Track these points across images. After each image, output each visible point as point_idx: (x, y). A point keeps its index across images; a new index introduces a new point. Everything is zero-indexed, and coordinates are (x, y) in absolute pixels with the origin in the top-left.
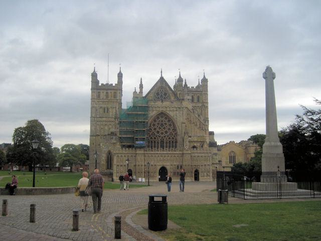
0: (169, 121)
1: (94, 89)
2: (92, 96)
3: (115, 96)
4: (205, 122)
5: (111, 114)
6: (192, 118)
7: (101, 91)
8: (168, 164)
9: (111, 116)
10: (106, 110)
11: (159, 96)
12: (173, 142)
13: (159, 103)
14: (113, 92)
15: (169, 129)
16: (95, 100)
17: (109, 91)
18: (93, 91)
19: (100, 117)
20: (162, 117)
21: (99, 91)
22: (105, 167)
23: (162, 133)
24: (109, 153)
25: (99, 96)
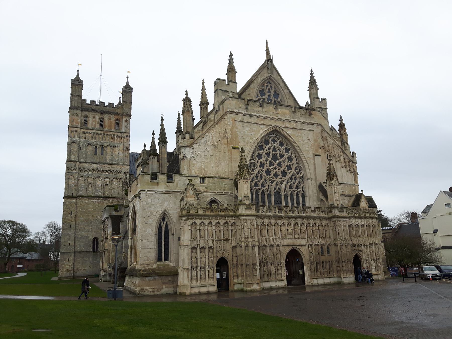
0: (287, 150)
1: (77, 109)
2: (71, 120)
3: (117, 126)
4: (353, 157)
5: (109, 157)
6: (330, 147)
7: (91, 115)
8: (304, 242)
9: (108, 162)
10: (99, 150)
11: (266, 97)
12: (297, 195)
13: (269, 110)
14: (113, 118)
15: (289, 167)
16: (79, 130)
17: (106, 117)
18: (75, 111)
19: (86, 163)
20: (274, 141)
21: (87, 113)
22: (153, 254)
23: (276, 175)
24: (164, 217)
25: (85, 124)
